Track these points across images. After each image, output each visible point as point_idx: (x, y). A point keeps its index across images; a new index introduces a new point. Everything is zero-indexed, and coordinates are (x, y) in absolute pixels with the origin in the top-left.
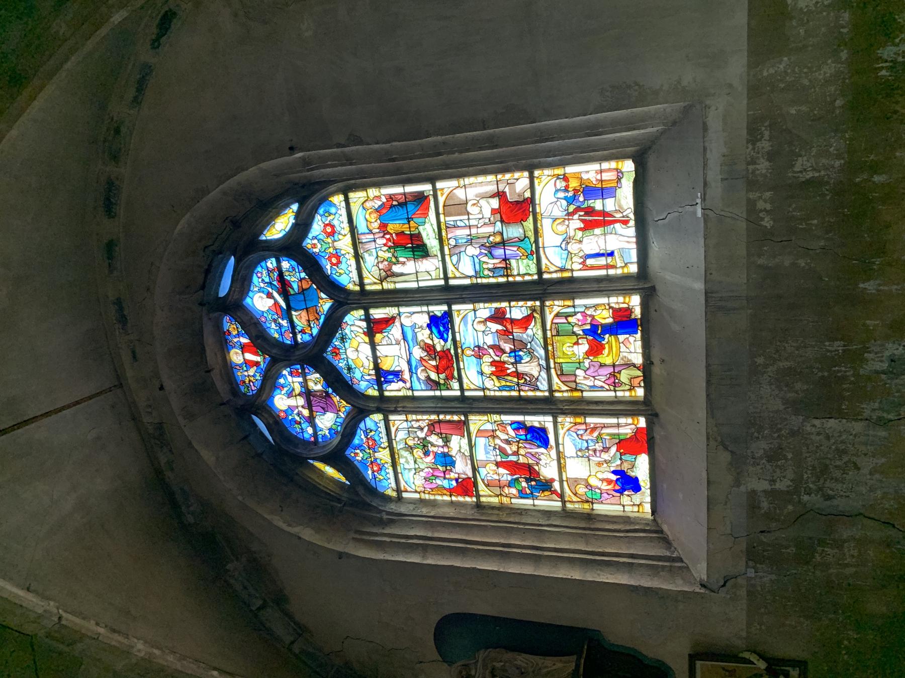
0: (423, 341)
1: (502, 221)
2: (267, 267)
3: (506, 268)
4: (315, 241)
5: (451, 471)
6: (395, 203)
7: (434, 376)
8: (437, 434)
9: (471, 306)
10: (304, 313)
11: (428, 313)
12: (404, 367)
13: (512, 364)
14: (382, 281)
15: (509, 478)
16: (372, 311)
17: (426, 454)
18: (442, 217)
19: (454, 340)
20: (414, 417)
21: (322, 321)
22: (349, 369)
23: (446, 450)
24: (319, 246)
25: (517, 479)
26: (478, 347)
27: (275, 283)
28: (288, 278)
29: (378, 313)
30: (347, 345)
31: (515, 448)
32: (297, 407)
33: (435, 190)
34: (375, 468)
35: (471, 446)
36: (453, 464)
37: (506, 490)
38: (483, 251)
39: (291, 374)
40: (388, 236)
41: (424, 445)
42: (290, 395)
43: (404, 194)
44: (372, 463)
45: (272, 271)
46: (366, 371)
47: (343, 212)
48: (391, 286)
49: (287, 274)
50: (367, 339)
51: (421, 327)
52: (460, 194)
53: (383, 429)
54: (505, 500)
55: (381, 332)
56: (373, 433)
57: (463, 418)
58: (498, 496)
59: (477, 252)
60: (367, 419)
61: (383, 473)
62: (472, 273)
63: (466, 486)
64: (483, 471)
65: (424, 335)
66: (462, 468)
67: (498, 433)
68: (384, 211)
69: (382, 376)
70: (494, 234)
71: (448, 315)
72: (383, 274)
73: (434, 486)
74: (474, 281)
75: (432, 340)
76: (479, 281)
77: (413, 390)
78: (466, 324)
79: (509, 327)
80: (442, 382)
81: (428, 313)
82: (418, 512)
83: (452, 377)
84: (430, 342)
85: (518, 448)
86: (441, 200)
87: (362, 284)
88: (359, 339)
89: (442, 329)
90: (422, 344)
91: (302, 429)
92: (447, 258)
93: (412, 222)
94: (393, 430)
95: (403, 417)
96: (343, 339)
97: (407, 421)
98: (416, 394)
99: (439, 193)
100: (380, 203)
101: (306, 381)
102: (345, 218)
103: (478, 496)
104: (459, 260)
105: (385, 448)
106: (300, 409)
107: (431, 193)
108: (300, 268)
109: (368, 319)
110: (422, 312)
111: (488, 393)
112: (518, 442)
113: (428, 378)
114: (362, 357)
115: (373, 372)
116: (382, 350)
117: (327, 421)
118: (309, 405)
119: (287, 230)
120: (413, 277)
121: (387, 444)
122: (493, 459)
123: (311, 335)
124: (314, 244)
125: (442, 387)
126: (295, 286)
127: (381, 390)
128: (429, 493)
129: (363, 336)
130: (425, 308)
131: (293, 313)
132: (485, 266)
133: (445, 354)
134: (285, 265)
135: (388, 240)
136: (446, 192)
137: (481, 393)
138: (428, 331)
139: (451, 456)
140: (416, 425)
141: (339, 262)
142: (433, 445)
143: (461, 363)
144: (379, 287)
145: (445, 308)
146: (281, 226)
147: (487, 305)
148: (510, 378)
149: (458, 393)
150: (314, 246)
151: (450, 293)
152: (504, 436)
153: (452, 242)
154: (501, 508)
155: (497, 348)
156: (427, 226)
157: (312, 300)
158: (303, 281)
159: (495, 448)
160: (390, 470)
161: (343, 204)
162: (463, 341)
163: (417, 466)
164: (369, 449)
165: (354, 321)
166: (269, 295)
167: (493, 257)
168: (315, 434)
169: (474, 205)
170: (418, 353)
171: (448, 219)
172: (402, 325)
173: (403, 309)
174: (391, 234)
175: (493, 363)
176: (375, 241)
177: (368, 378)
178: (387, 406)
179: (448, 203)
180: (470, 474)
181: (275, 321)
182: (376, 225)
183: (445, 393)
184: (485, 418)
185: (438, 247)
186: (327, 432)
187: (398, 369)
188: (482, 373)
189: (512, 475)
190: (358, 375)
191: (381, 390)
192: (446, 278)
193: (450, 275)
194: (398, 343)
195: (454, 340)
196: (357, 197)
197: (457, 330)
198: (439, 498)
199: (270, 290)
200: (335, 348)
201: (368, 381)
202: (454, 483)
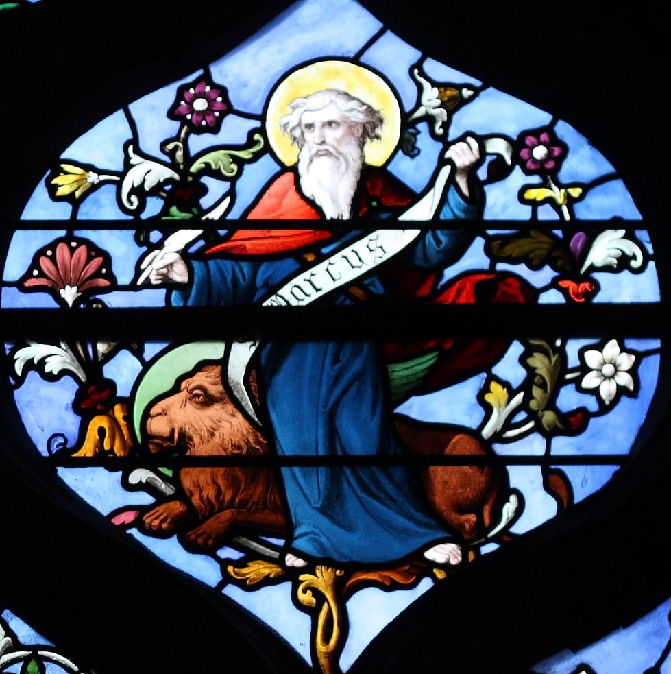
2: (594, 229)
27: (475, 257)
28: (509, 367)
45: (570, 264)
49: (539, 362)
126: (450, 406)
134: (608, 364)
166: (379, 197)
181: (184, 192)
199: (423, 211)
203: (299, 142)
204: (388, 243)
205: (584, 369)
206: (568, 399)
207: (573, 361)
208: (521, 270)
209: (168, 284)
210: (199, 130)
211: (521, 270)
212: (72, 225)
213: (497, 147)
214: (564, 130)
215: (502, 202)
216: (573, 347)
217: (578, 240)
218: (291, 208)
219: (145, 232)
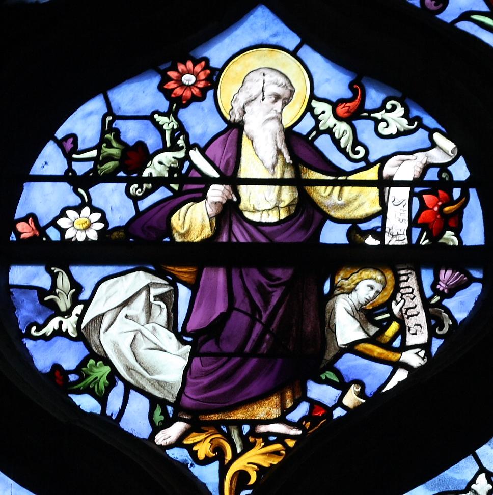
39: (431, 186)
42: (299, 147)
101: (388, 259)
106: (217, 193)
118: (233, 248)
168: (63, 255)
186: (69, 324)
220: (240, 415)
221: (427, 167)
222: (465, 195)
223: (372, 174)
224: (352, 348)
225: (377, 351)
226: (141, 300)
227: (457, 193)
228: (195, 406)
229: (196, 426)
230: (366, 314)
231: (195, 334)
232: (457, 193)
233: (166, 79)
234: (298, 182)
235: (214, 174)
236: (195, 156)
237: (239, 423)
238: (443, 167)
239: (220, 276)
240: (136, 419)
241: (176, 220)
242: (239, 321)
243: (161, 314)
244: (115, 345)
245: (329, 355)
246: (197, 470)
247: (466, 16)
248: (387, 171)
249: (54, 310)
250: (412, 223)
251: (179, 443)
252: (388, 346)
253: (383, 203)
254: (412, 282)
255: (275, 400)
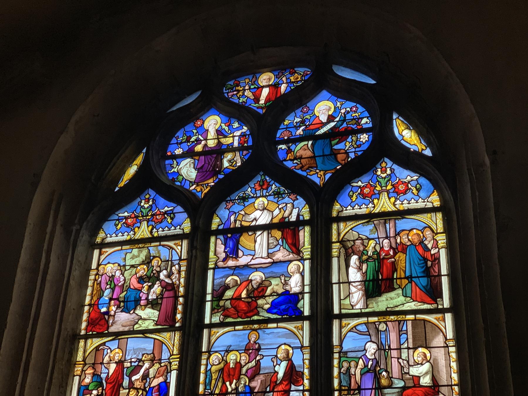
0: (271, 284)
1: (404, 388)
2: (362, 118)
3: (349, 389)
4: (389, 172)
5: (119, 307)
6: (429, 263)
7: (229, 294)
8: (162, 294)
9: (306, 343)
10: (309, 153)
11: (302, 293)
12: (243, 260)
13: (237, 388)
14: (342, 242)
15: (104, 376)
16: (307, 229)
17: (141, 280)
18: (412, 317)
19: (269, 321)
20: (183, 268)
21: (300, 172)
22: (244, 199)
23: (143, 302)
24: (384, 175)
25: (101, 385)
26: (259, 349)
27: (345, 125)
28: (349, 139)
29: (305, 235)
30: (271, 198)
31: (138, 384)
32: (206, 139)
33: (443, 311)
34: (129, 221)
35: (144, 332)
36: (126, 310)
37: (90, 371)
38: (370, 363)
39: (243, 135)
40: (391, 253)
41: (152, 278)
42: (220, 133)
43: (440, 275)
44: (137, 217)
45: (358, 123)
46: (240, 217)
47: (421, 205)
48: (335, 252)
49: (354, 138)
50: (276, 221)
51: (286, 283)
52: (439, 341)
53: (173, 231)
54: (78, 369)
55: (283, 238)
56: (169, 220)
57: (177, 325)
58: (84, 360)
59: (369, 355)
60: (185, 215)
61: (125, 229)
62: (345, 348)
63: (100, 325)
64: (114, 345)
65: (276, 285)
66: (121, 320)
67: (157, 366)
68: (421, 251)
69: (234, 235)
70: (390, 378)
71: (299, 316)
72: (349, 244)
73: (103, 286)
74: (335, 350)
75: (271, 295)
76: (336, 356)
77: (214, 269)
78: (285, 336)
79: (280, 388)
80: (222, 303)
81: (302, 293)
82: (75, 266)
83: (226, 316)
84: (269, 291)
85: (137, 389)
86: (430, 318)
87: (340, 219)
88: (277, 212)
89: (283, 307)
90: (267, 283)
91: (181, 143)
92: (364, 320)
93: (407, 281)
94: (171, 244)
95: (184, 256)
96: (277, 194)
97: (180, 259)
98: (210, 273)
99: (440, 316)
100: (430, 246)
102: (413, 205)
103: (86, 337)
104: (361, 333)
105: (151, 232)
106: (203, 143)
107: (440, 307)
108: (359, 153)
109: (300, 223)
110: (303, 285)
111: (204, 357)
112: (144, 389)
113: (227, 287)
114: (257, 214)
115: (238, 225)
116: (262, 238)
117: (187, 170)
118: (207, 152)
119: (402, 142)
120: (343, 278)
121: (156, 235)
122: (128, 358)
123: (285, 160)
124: (386, 171)
125: (215, 303)
127: (217, 233)
128: (95, 280)
129: (280, 216)
130: (307, 289)
131: (310, 142)
132: (353, 364)
133: (254, 309)
134: (364, 138)
135: (387, 253)
136: (441, 325)
137: (204, 349)
138: (281, 291)
139: (135, 309)
140: (174, 269)
141: (364, 196)
142: (150, 288)
143: (241, 327)
144: (334, 238)
145: (307, 313)
146: (408, 136)
147: (307, 362)
148: (220, 384)
149: (207, 321)
150: (384, 171)
151: (323, 319)
152: (152, 372)
153: (382, 327)
154: (71, 363)
155: (256, 371)
156: (402, 299)
157: (323, 163)
158: (344, 156)
159: (140, 360)
160: (126, 237)
161: (429, 205)
162: (268, 331)
163: (127, 268)
164: (152, 215)
165: (298, 209)
166: (331, 118)
167: (361, 375)
168: (174, 157)
169: (425, 356)
170: (257, 277)
171: (410, 324)
172: (290, 261)
173: (307, 263)
174: (393, 257)
175: (239, 365)
176: (387, 238)
177: (232, 218)
178: (198, 240)
179: (428, 326)
180: (112, 329)
181: (303, 122)
182: (405, 240)
183: (208, 306)
184: (175, 352)
185: (377, 310)
186: (176, 170)
187: (240, 253)
188: (228, 351)
189: (107, 378)
190: (236, 208)
191: (217, 233)
192: (341, 316)
193: (344, 322)
194: (269, 255)
195: (269, 321)
196: (437, 221)
197: (280, 325)
198: (89, 291)
199: (337, 119)
200: (269, 185)
201: (229, 218)
202: (104, 310)
203: (319, 113)
204: (332, 124)
205: (360, 138)
206: (358, 143)
207: (359, 137)
208: (351, 126)
209: (300, 135)
210: (304, 113)
211: (351, 126)
212: (287, 128)
213: (348, 109)
214: (358, 105)
215: (348, 117)
216: (359, 136)
217: (360, 121)
218: (318, 122)
219: (297, 128)
220: (206, 182)
221: (242, 133)
222: (249, 137)
223: (231, 135)
224: (227, 168)
225: (231, 167)
226: (189, 164)
227: (247, 136)
228: (197, 182)
229: (198, 185)
230: (229, 161)
231: (198, 169)
232: (247, 136)
233: (195, 123)
234: (218, 139)
235: (202, 139)
236: (200, 137)
237: (205, 184)
238: (245, 132)
239: (203, 157)
240: (187, 186)
241: (196, 149)
242: (207, 165)
243: (192, 166)
244: (184, 173)
245: (222, 169)
246: (197, 193)
247: (250, 105)
248: (234, 134)
249: (173, 167)
250: (239, 143)
251: (194, 189)
252: (233, 166)
253: (233, 140)
254: (238, 154)
255: (212, 179)
